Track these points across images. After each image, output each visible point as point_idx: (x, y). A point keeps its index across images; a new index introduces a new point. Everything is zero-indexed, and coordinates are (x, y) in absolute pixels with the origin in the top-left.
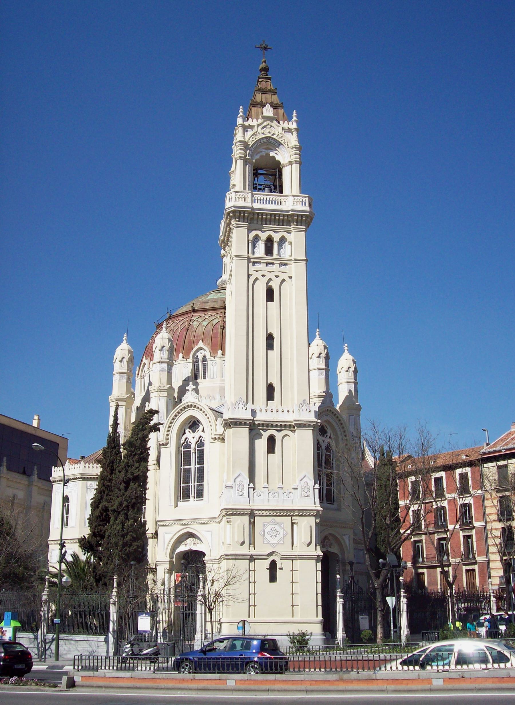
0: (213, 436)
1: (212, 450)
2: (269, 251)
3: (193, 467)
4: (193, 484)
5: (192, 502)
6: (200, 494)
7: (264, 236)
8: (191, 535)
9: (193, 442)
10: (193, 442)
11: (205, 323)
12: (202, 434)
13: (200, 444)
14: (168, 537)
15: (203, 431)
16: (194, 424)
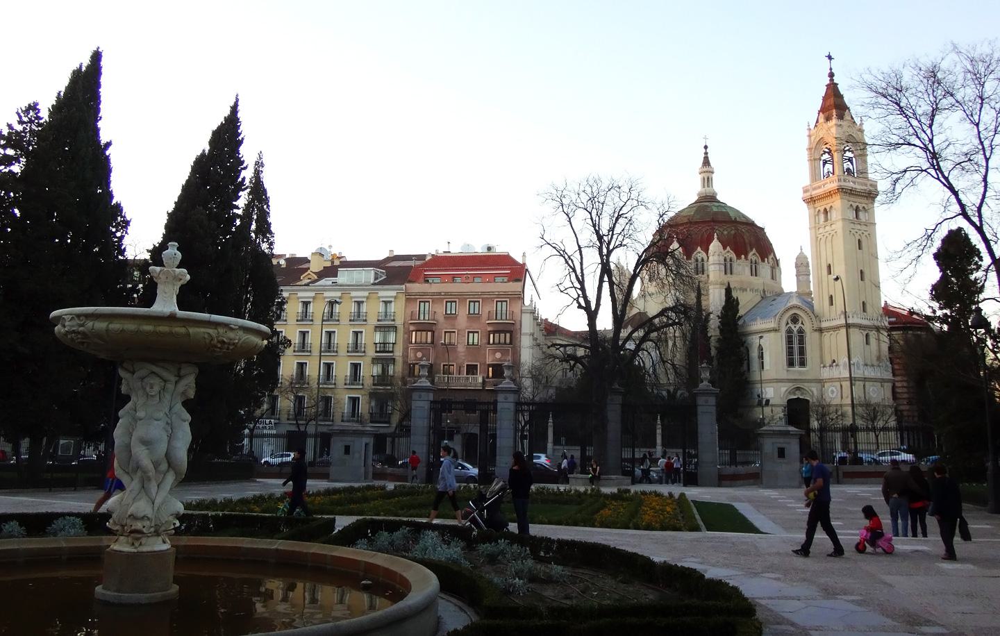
0: (815, 328)
1: (811, 339)
2: (857, 217)
3: (796, 346)
4: (796, 357)
5: (797, 368)
6: (803, 364)
7: (855, 205)
8: (798, 389)
9: (795, 330)
10: (795, 330)
11: (725, 233)
12: (802, 326)
13: (801, 331)
14: (784, 389)
15: (802, 323)
16: (795, 319)
